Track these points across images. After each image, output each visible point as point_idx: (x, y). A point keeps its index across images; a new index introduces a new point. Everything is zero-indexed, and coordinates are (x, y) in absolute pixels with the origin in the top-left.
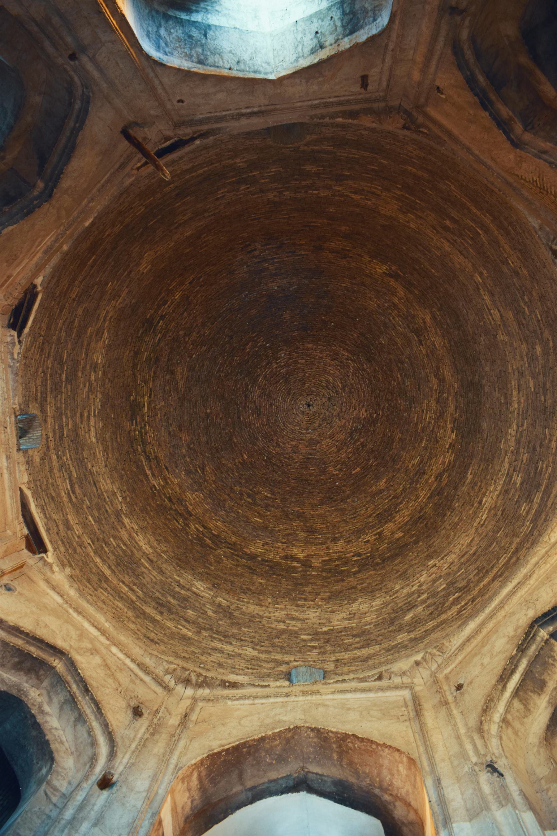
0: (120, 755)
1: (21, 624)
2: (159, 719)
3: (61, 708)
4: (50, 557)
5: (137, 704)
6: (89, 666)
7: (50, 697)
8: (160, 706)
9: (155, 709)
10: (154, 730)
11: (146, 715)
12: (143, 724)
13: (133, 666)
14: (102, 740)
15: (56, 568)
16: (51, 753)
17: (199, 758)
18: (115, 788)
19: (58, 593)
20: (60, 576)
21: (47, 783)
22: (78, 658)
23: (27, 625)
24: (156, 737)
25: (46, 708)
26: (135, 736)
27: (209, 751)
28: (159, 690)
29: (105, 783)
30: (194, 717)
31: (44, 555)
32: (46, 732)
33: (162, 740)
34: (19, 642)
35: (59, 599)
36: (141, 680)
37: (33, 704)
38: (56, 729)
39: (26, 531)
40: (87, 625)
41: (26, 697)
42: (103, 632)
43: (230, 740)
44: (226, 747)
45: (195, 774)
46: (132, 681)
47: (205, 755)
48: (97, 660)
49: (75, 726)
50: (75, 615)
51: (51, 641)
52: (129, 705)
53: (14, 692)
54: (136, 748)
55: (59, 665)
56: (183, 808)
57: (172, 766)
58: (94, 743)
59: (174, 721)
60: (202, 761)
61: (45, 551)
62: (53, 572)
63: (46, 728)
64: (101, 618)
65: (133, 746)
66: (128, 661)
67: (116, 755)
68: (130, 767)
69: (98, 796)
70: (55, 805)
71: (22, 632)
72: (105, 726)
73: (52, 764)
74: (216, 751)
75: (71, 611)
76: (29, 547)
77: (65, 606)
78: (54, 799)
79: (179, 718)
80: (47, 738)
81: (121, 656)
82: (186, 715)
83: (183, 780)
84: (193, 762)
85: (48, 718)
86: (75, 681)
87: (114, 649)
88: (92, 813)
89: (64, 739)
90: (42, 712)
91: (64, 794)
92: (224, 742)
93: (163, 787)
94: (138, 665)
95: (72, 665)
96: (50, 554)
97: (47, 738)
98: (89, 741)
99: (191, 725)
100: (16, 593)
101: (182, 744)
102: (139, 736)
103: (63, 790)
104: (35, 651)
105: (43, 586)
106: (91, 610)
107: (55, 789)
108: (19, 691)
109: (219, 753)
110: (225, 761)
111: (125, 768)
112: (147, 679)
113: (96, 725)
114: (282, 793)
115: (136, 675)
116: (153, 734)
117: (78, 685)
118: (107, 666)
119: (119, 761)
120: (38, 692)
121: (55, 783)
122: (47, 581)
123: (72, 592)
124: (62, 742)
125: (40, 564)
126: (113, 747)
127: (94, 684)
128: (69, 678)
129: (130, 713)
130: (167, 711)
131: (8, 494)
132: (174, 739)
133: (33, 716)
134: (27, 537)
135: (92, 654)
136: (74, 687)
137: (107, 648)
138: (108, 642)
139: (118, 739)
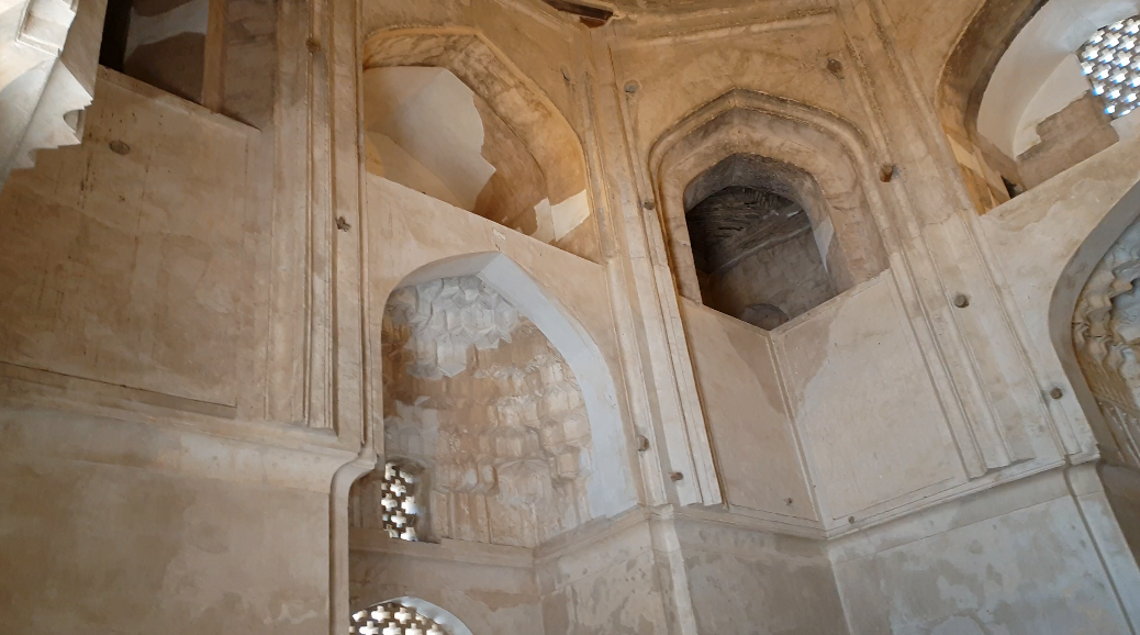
0: (867, 131)
1: (681, 113)
2: (862, 58)
3: (770, 127)
4: (619, 14)
5: (825, 59)
6: (758, 75)
7: (750, 127)
8: (847, 40)
9: (843, 45)
10: (867, 73)
11: (843, 63)
12: (849, 71)
13: (784, 24)
14: (835, 128)
15: (633, 17)
16: (802, 170)
17: (941, 74)
18: (900, 167)
19: (661, 36)
20: (643, 20)
21: (829, 199)
22: (745, 80)
23: (684, 107)
24: (878, 82)
25: (757, 136)
26: (859, 98)
27: (944, 57)
28: (826, 19)
29: (887, 177)
30: (887, 22)
31: (613, 18)
32: (780, 157)
33: (883, 74)
34: (692, 124)
35: (666, 41)
36: (803, 27)
37: (746, 146)
38: (782, 145)
39: (577, 18)
40: (712, 35)
41: (734, 146)
42: (732, 24)
43: (955, 30)
44: (958, 41)
45: (947, 88)
46: (799, 40)
47: (944, 66)
48: (757, 59)
49: (798, 132)
50: (693, 37)
51: (714, 95)
52: (824, 70)
53: (724, 155)
54: (873, 108)
55: (736, 102)
56: (957, 122)
57: (922, 103)
58: (833, 136)
59: (874, 46)
60: (945, 74)
61: (608, 14)
62: (634, 22)
63: (775, 154)
64: (716, 12)
65: (868, 109)
66: (776, 25)
67: (866, 136)
68: (891, 140)
69: (893, 189)
70: (851, 209)
71: (688, 117)
72: (829, 116)
73: (812, 178)
74: (950, 53)
75: (687, 38)
76: (592, 24)
77: (678, 40)
78: (846, 205)
79: (876, 37)
80: (786, 162)
81: (765, 27)
82: (879, 28)
83: (942, 106)
84: (938, 82)
85: (767, 144)
86: (764, 102)
87: (755, 28)
88: (904, 210)
89: (796, 146)
90: (759, 144)
91: (847, 193)
92: (950, 36)
93: (936, 133)
94: (788, 18)
95: (747, 92)
96: (616, 12)
97: (786, 162)
98: (825, 136)
99: (893, 35)
100: (640, 85)
101: (906, 67)
102: (861, 93)
103: (843, 190)
104: (710, 115)
105: (643, 45)
106: (699, 15)
107: (838, 196)
108: (724, 148)
109: (955, 52)
110: (964, 51)
111: (887, 144)
112: (807, 21)
113: (817, 120)
114: (1033, 15)
115: (795, 29)
116: (873, 83)
117: (770, 103)
118: (769, 55)
119: (873, 139)
120: (736, 130)
121: (832, 191)
122: (641, 37)
123: (669, 19)
124: (799, 151)
125: (617, 27)
126: (855, 129)
127: (782, 89)
128: (756, 103)
129: (831, 78)
130: (858, 39)
131: (536, 16)
132: (896, 69)
133: (757, 156)
134: (582, 20)
135: (748, 60)
136: (767, 106)
137: (748, 34)
138: (744, 28)
139: (853, 119)
